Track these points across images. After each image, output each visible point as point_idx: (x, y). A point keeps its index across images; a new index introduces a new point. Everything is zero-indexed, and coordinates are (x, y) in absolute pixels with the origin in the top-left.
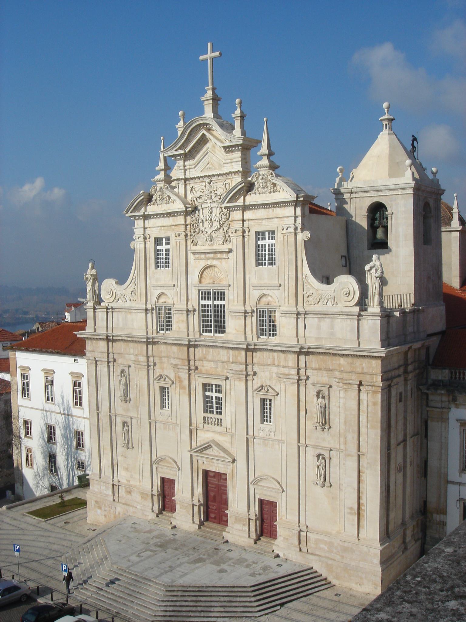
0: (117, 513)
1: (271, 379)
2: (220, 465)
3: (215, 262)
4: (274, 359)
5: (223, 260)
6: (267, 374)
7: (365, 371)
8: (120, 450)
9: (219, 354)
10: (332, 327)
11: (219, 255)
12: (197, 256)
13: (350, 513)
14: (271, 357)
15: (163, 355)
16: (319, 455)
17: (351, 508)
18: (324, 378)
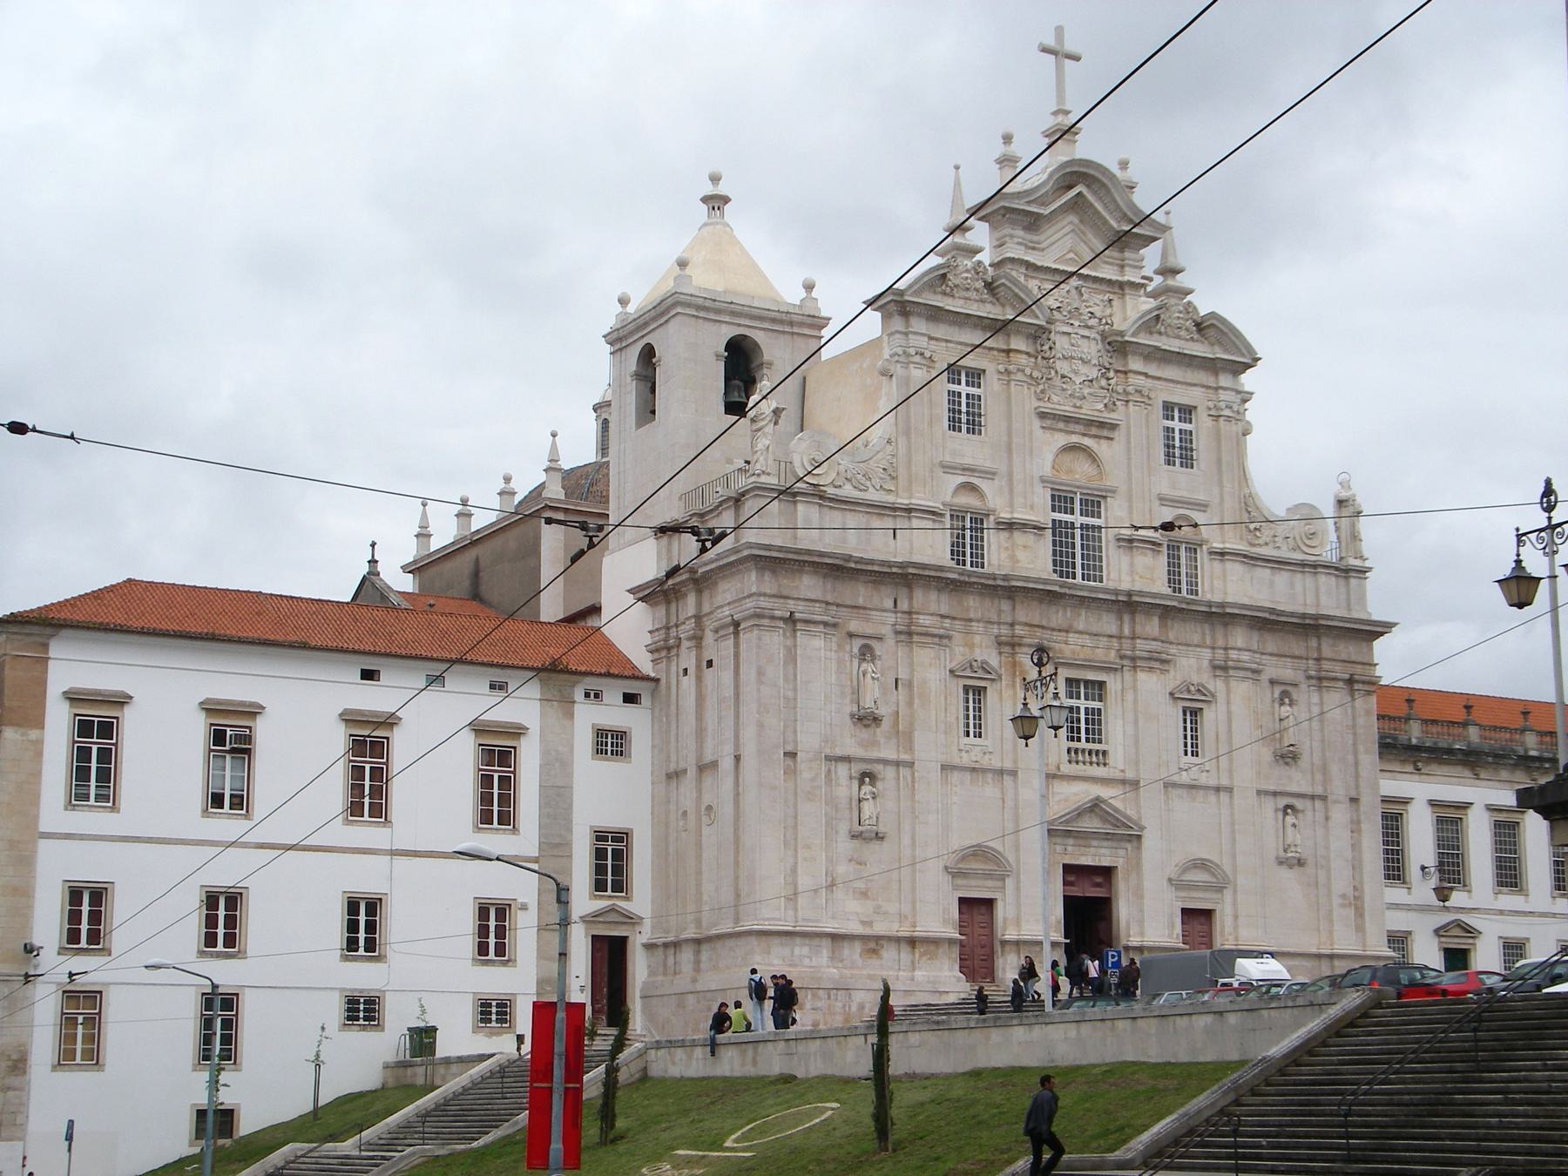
0: (854, 1008)
1: (1199, 669)
2: (1103, 851)
3: (1087, 441)
4: (1204, 634)
6: (1192, 661)
7: (1353, 658)
8: (844, 845)
10: (1292, 585)
11: (1094, 431)
12: (1048, 423)
13: (1343, 906)
15: (972, 616)
16: (1287, 806)
17: (1344, 896)
18: (1286, 671)
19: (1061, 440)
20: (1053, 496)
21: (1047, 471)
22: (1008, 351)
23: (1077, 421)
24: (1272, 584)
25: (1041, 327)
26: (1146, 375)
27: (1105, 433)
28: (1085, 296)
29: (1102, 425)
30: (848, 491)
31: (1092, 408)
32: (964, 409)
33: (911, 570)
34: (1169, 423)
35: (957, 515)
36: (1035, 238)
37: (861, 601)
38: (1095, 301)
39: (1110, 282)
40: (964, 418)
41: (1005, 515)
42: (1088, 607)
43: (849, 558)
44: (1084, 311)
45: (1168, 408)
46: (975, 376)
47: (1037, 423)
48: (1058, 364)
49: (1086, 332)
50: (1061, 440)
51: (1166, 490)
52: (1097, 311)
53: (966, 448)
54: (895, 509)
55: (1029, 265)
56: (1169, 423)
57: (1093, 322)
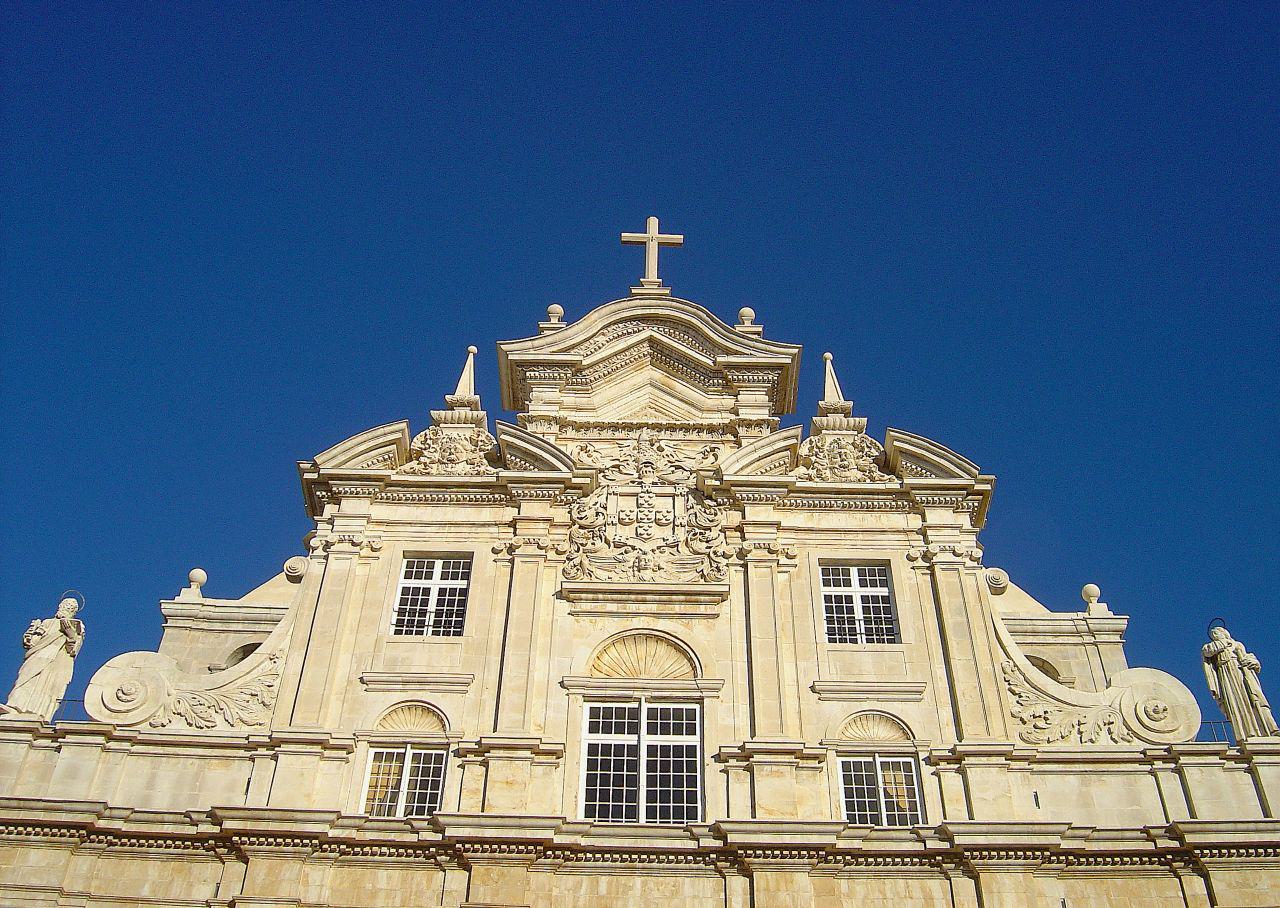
5: (695, 621)
9: (675, 893)
11: (677, 608)
14: (917, 894)
19: (613, 626)
20: (594, 712)
21: (580, 665)
22: (513, 524)
23: (641, 595)
24: (1085, 801)
25: (567, 485)
26: (778, 525)
27: (702, 609)
28: (668, 451)
29: (691, 596)
30: (178, 727)
31: (670, 576)
32: (432, 606)
33: (228, 825)
34: (842, 591)
35: (388, 752)
36: (582, 401)
37: (146, 892)
38: (691, 454)
39: (711, 429)
40: (430, 619)
41: (470, 738)
42: (648, 872)
43: (103, 809)
44: (661, 464)
45: (834, 571)
46: (460, 564)
47: (564, 606)
48: (610, 533)
49: (670, 490)
50: (613, 626)
51: (830, 674)
52: (688, 464)
53: (428, 653)
54: (251, 747)
55: (563, 424)
56: (842, 591)
57: (679, 474)
